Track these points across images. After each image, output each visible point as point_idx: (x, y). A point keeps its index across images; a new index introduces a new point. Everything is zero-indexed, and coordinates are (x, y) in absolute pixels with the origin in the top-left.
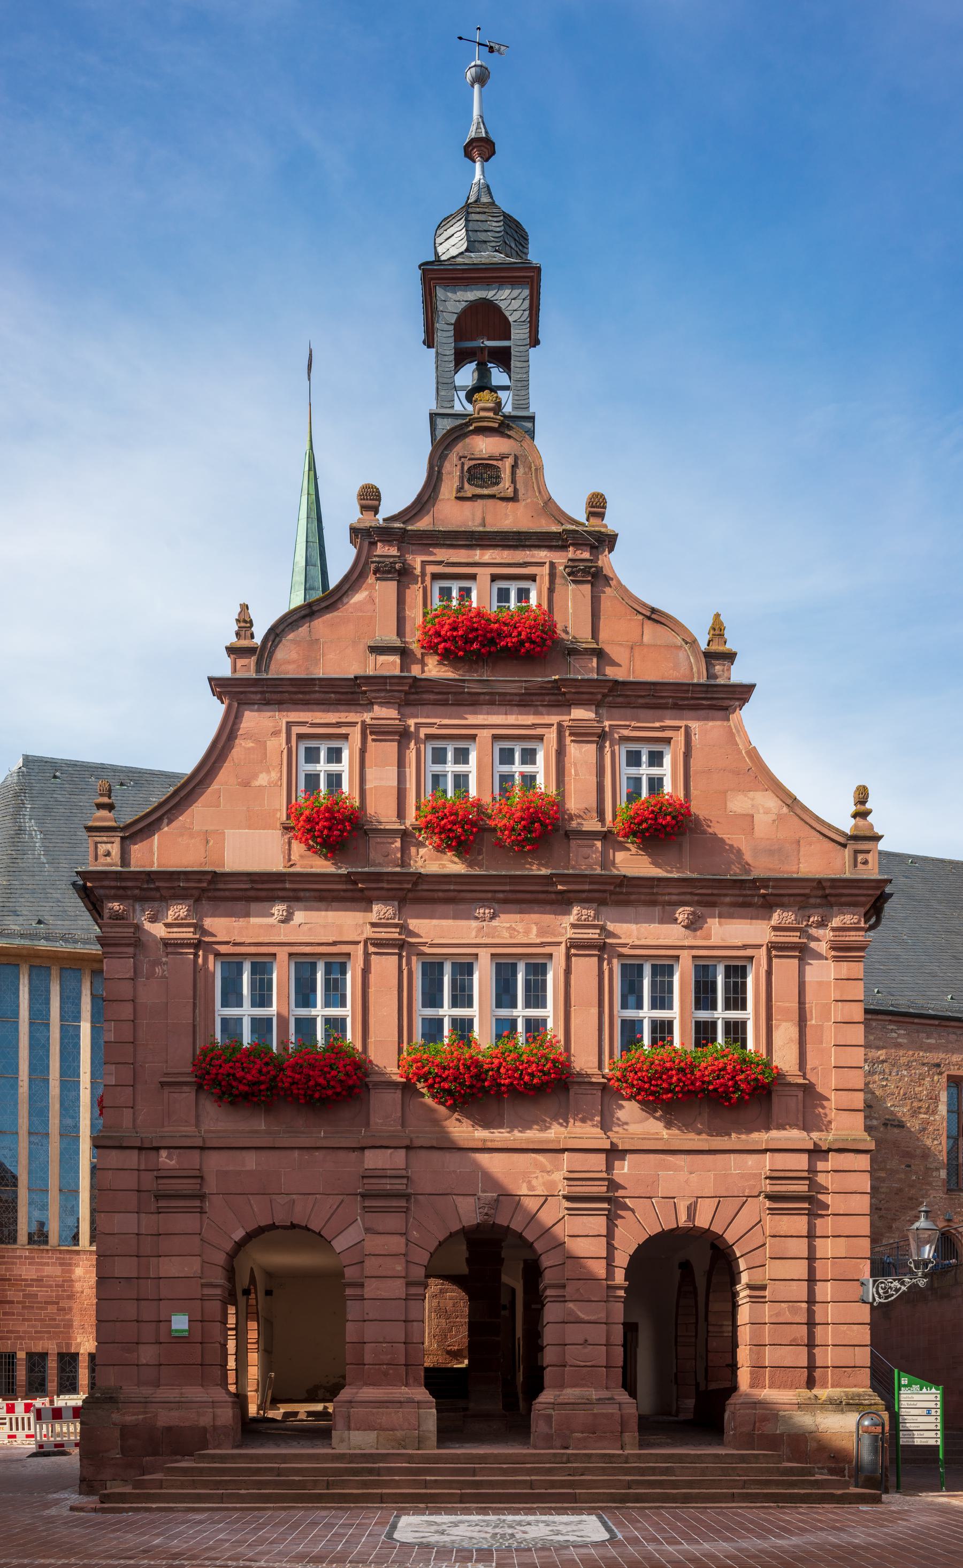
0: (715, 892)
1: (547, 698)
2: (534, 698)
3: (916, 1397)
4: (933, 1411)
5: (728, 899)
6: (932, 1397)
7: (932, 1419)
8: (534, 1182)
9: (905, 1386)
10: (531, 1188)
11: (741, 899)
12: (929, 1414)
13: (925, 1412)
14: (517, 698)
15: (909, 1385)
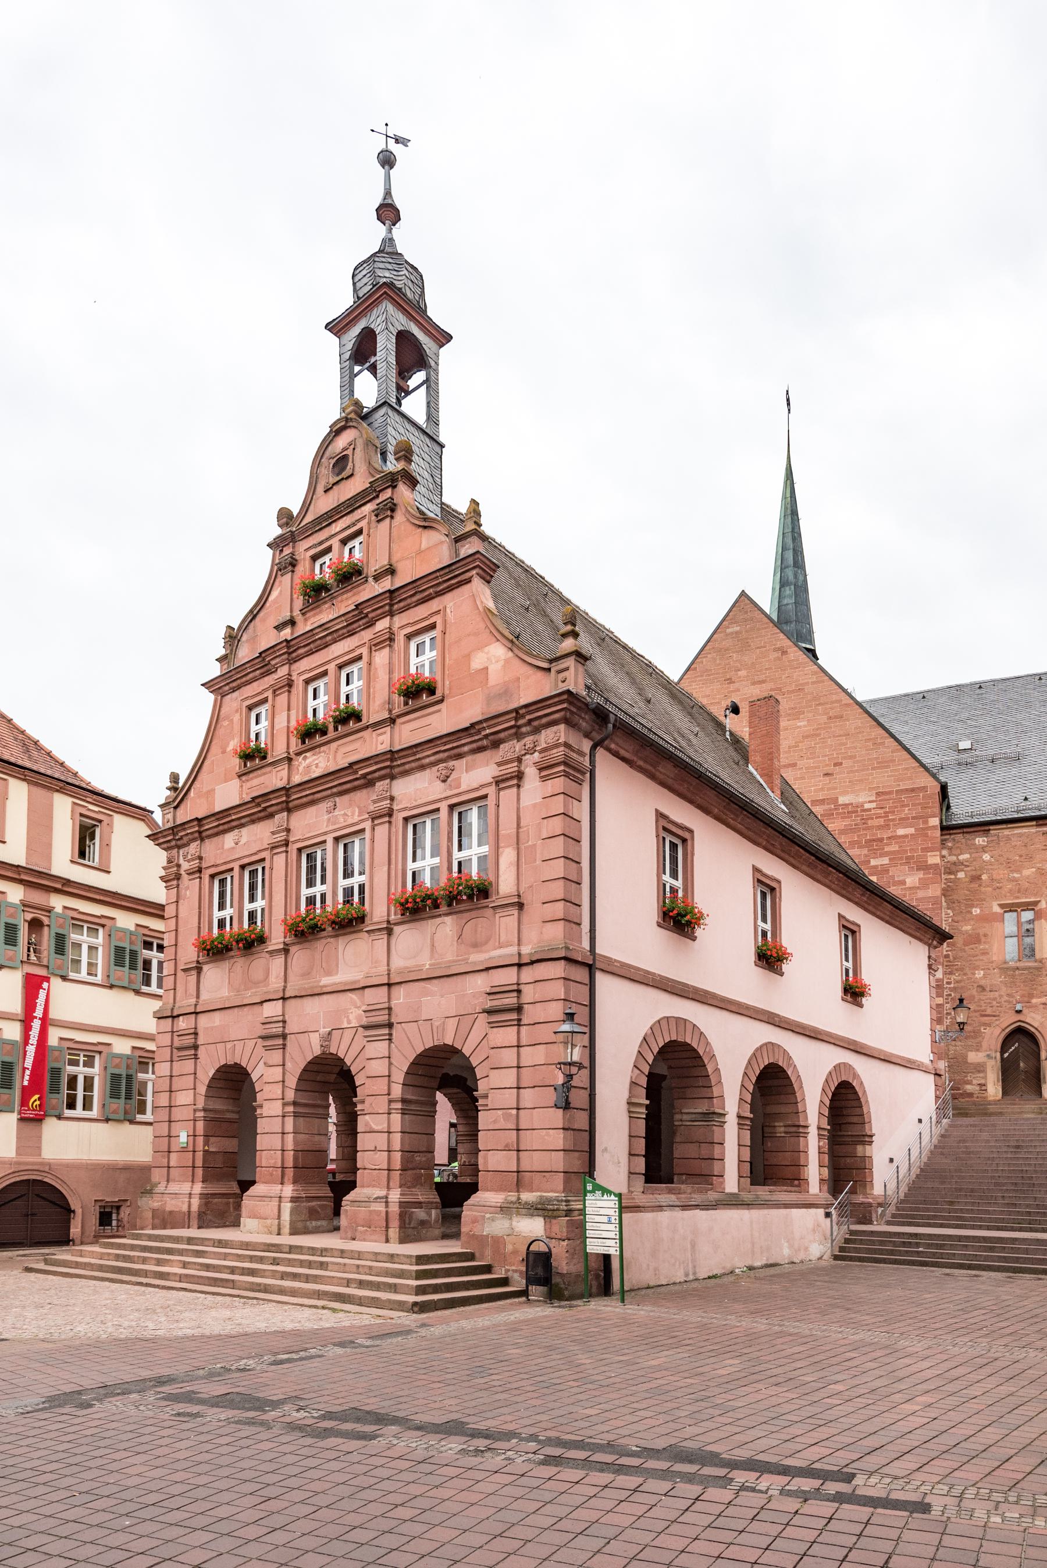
0: (455, 745)
1: (361, 623)
2: (354, 626)
3: (600, 1204)
4: (613, 1218)
5: (466, 749)
6: (611, 1204)
7: (611, 1227)
8: (351, 1017)
9: (590, 1192)
10: (349, 1022)
11: (474, 746)
12: (609, 1222)
13: (605, 1219)
14: (345, 631)
15: (593, 1191)
